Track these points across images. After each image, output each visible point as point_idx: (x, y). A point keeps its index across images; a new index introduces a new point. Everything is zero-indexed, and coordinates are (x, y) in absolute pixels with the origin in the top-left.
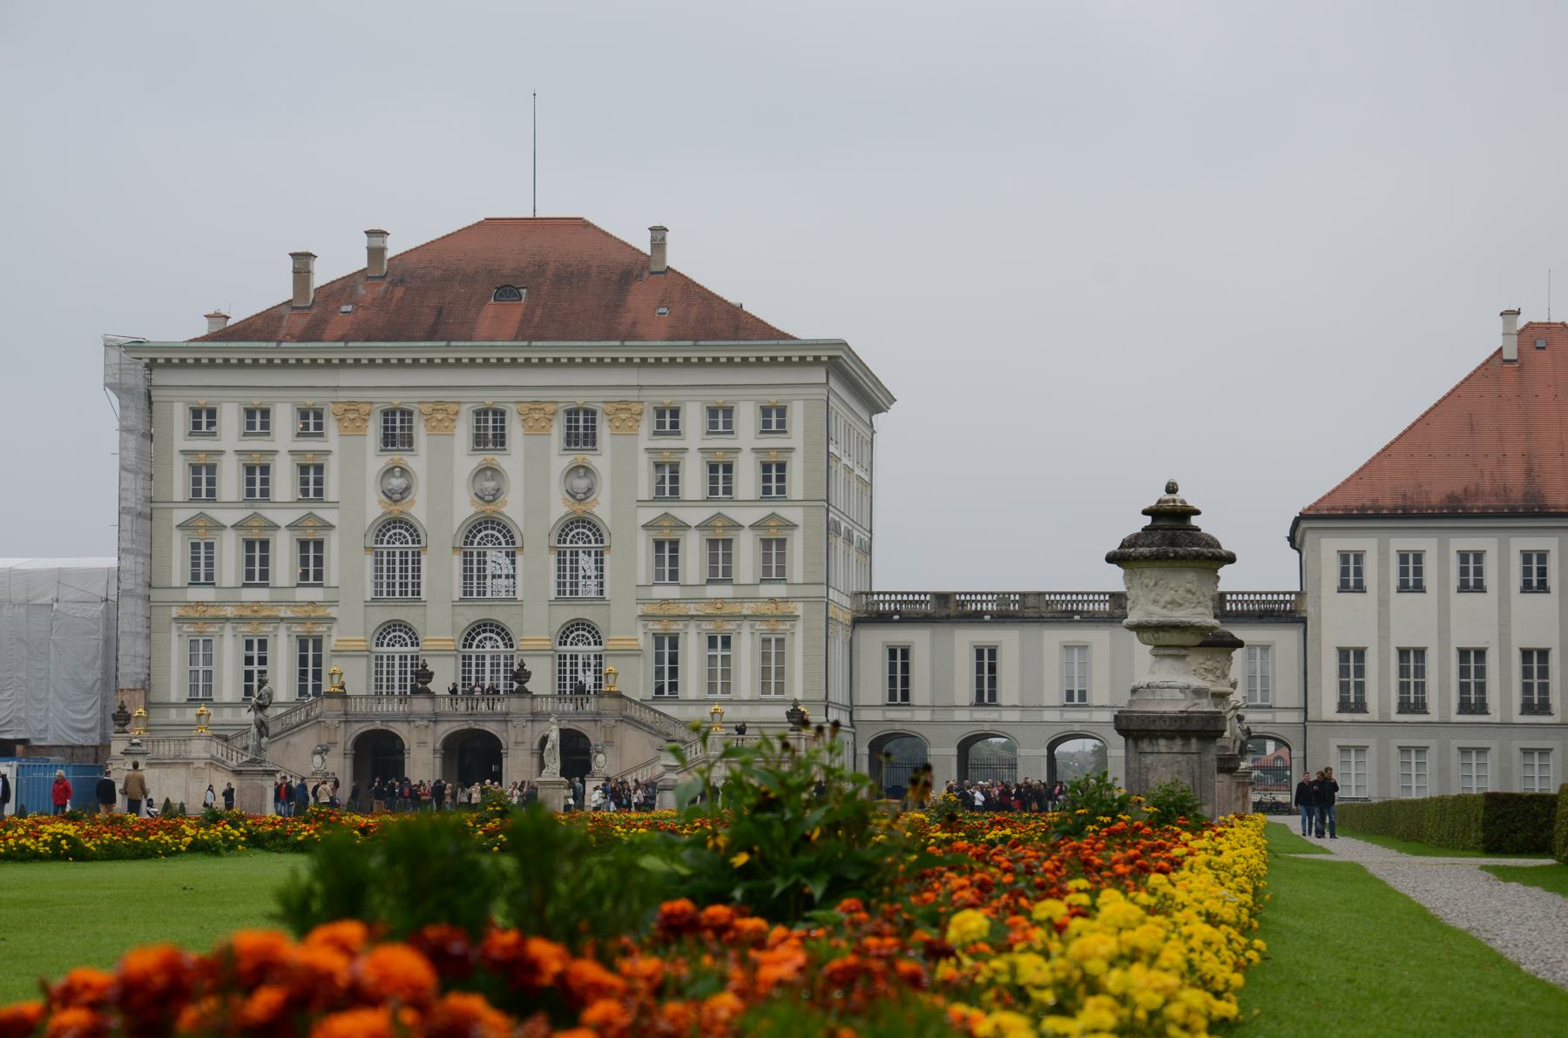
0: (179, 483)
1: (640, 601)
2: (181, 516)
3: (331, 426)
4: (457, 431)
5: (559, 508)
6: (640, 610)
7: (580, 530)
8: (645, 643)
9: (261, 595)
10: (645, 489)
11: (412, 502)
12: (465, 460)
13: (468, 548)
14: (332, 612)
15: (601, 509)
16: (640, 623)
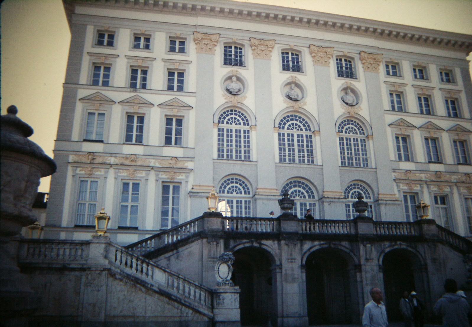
0: (85, 76)
1: (394, 170)
2: (82, 93)
3: (191, 47)
4: (272, 58)
5: (339, 110)
6: (394, 175)
7: (351, 124)
8: (399, 196)
9: (137, 150)
10: (386, 105)
11: (245, 98)
12: (280, 77)
13: (281, 131)
14: (190, 165)
15: (364, 111)
16: (395, 184)
